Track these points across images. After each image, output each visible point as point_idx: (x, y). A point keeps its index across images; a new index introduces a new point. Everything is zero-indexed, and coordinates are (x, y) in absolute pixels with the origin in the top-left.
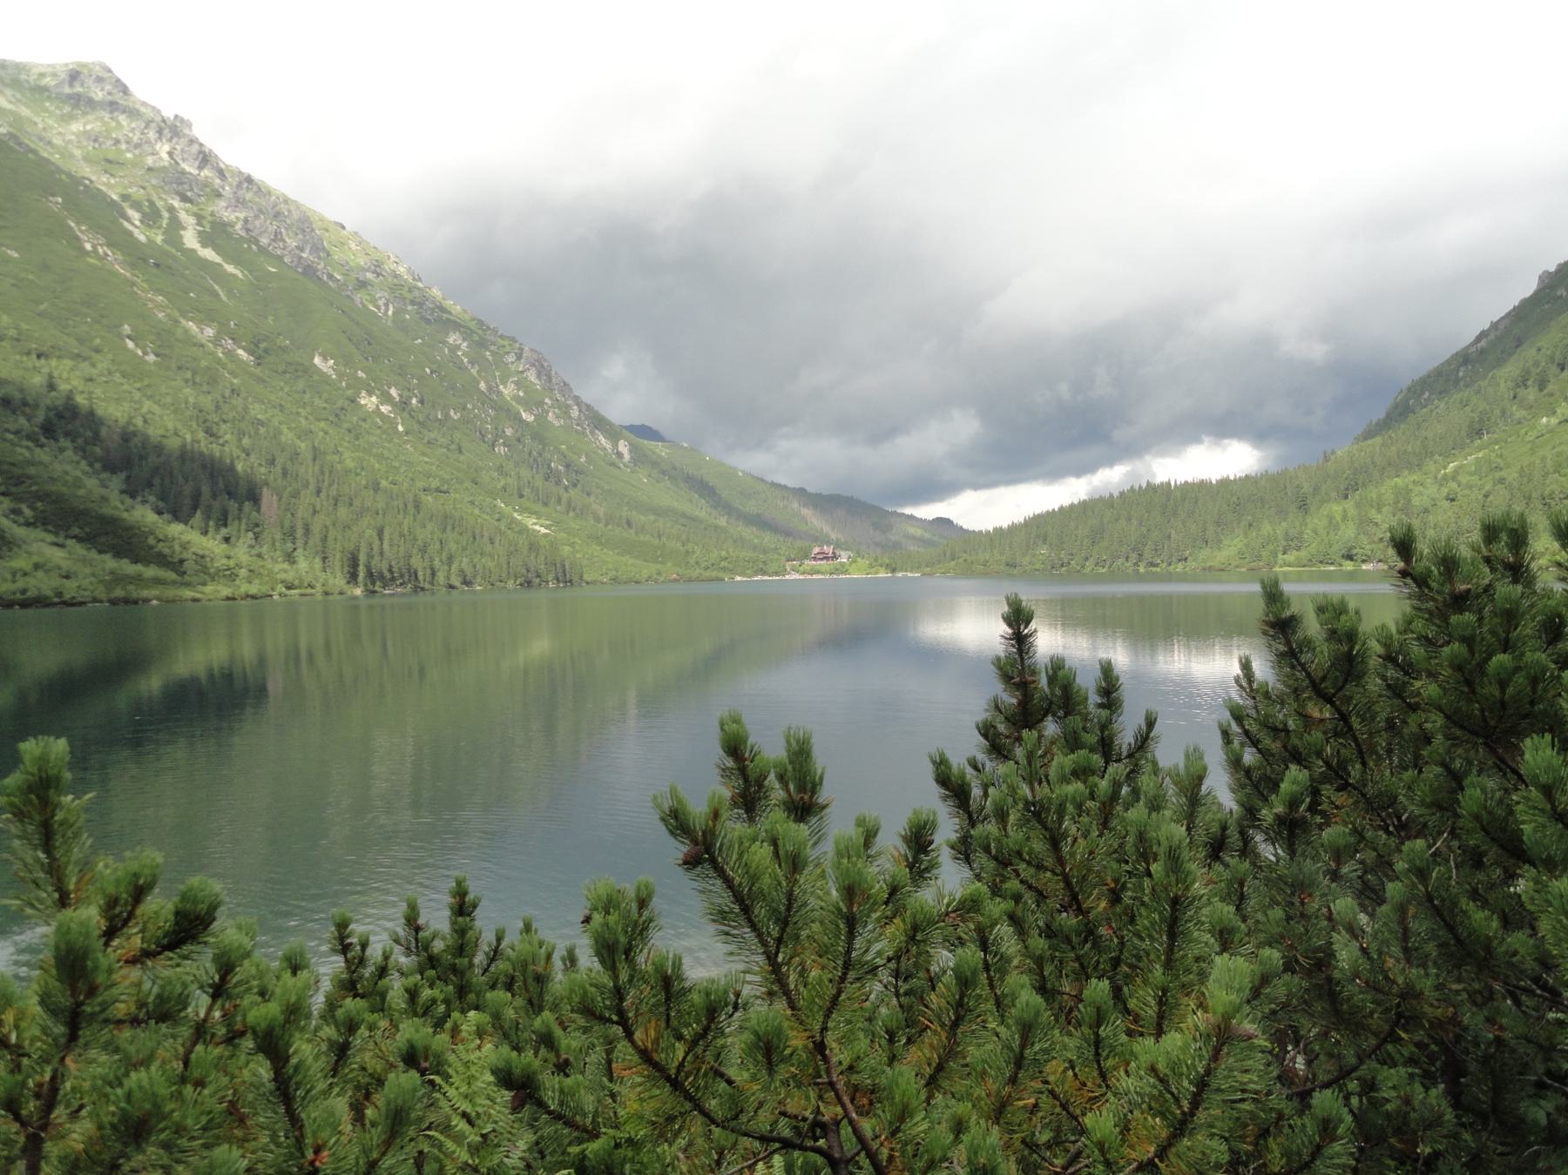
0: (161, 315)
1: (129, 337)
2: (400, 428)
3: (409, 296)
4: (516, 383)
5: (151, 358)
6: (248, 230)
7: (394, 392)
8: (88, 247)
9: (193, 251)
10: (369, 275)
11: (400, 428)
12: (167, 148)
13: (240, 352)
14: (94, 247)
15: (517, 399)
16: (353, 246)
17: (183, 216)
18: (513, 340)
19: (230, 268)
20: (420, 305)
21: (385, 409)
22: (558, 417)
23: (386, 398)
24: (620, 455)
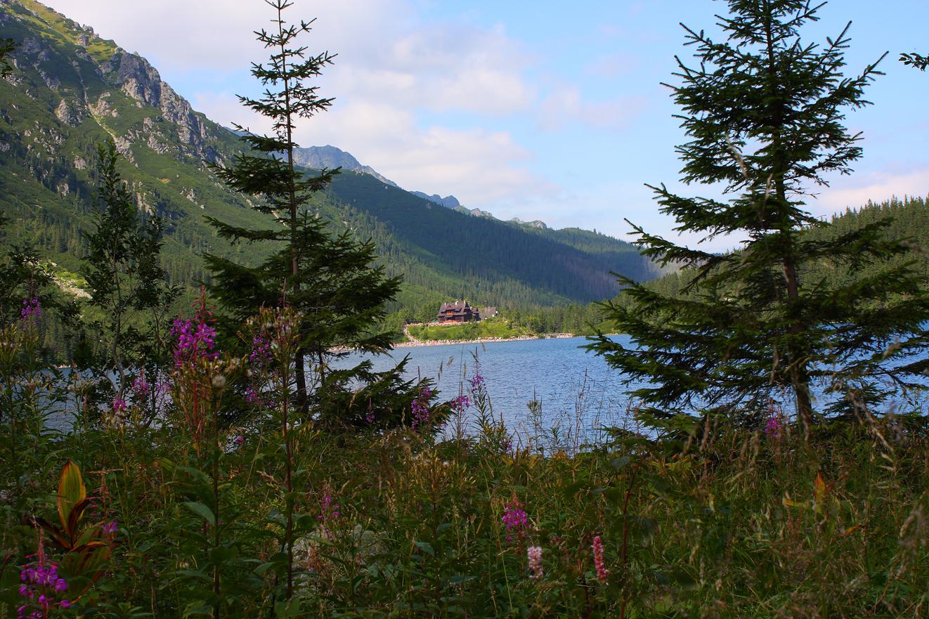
15: (109, 121)
22: (161, 142)
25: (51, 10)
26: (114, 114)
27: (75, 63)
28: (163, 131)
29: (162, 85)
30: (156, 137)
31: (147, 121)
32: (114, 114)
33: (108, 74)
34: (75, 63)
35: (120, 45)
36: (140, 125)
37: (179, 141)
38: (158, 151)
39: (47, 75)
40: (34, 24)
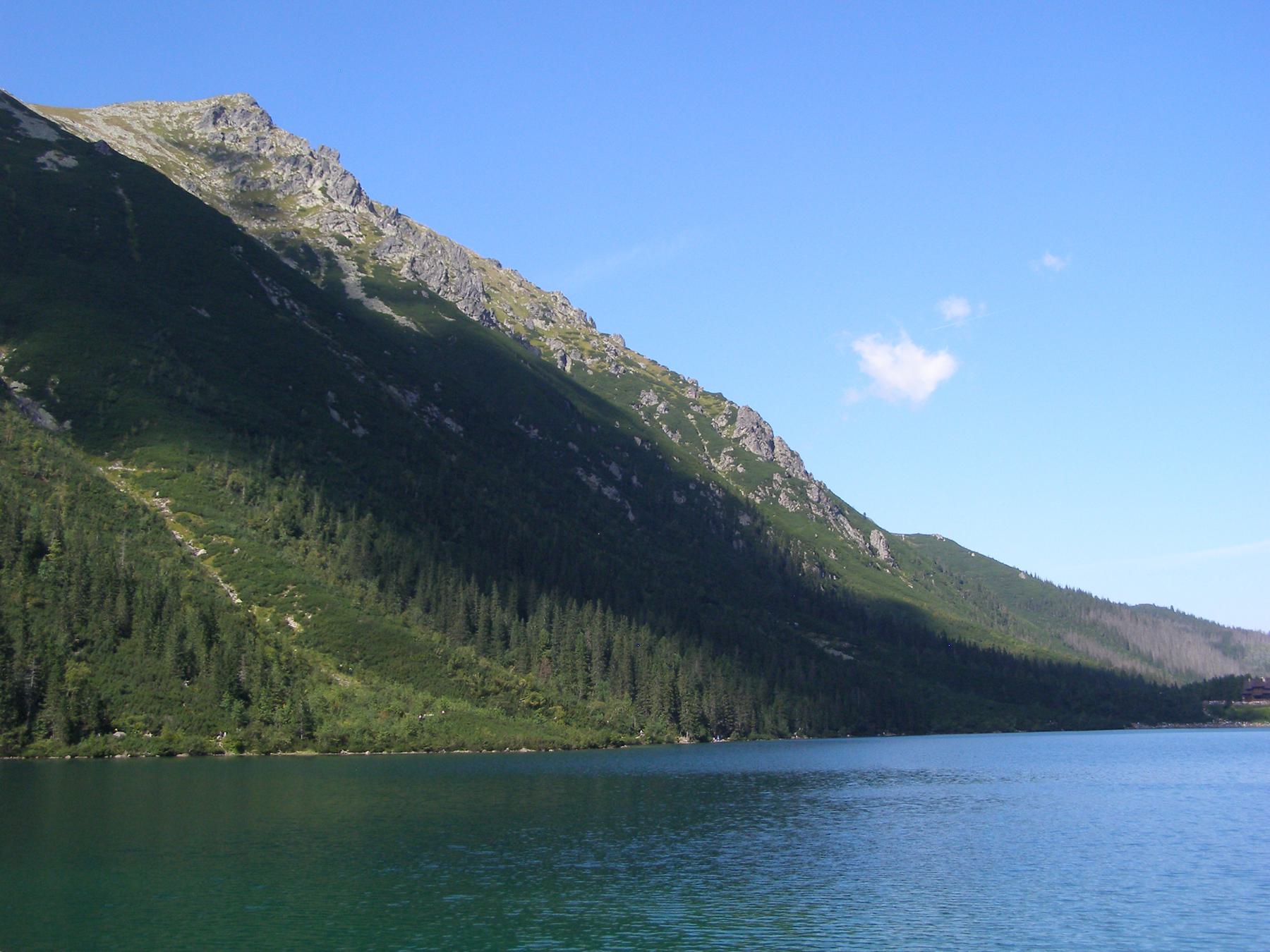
0: (361, 378)
1: (334, 406)
2: (631, 517)
3: (588, 347)
4: (732, 454)
5: (360, 431)
6: (415, 273)
7: (614, 468)
8: (275, 301)
9: (359, 302)
10: (538, 323)
11: (631, 517)
12: (319, 184)
13: (448, 421)
14: (280, 300)
15: (734, 475)
16: (515, 287)
17: (342, 260)
18: (720, 397)
19: (402, 320)
20: (603, 356)
21: (609, 491)
22: (792, 499)
23: (608, 478)
24: (874, 551)
25: (655, 362)
26: (740, 470)
27: (690, 416)
28: (793, 487)
29: (776, 441)
30: (787, 494)
31: (776, 477)
32: (740, 470)
33: (723, 428)
34: (690, 416)
35: (729, 399)
36: (770, 481)
37: (808, 499)
38: (791, 508)
39: (669, 428)
40: (645, 377)
